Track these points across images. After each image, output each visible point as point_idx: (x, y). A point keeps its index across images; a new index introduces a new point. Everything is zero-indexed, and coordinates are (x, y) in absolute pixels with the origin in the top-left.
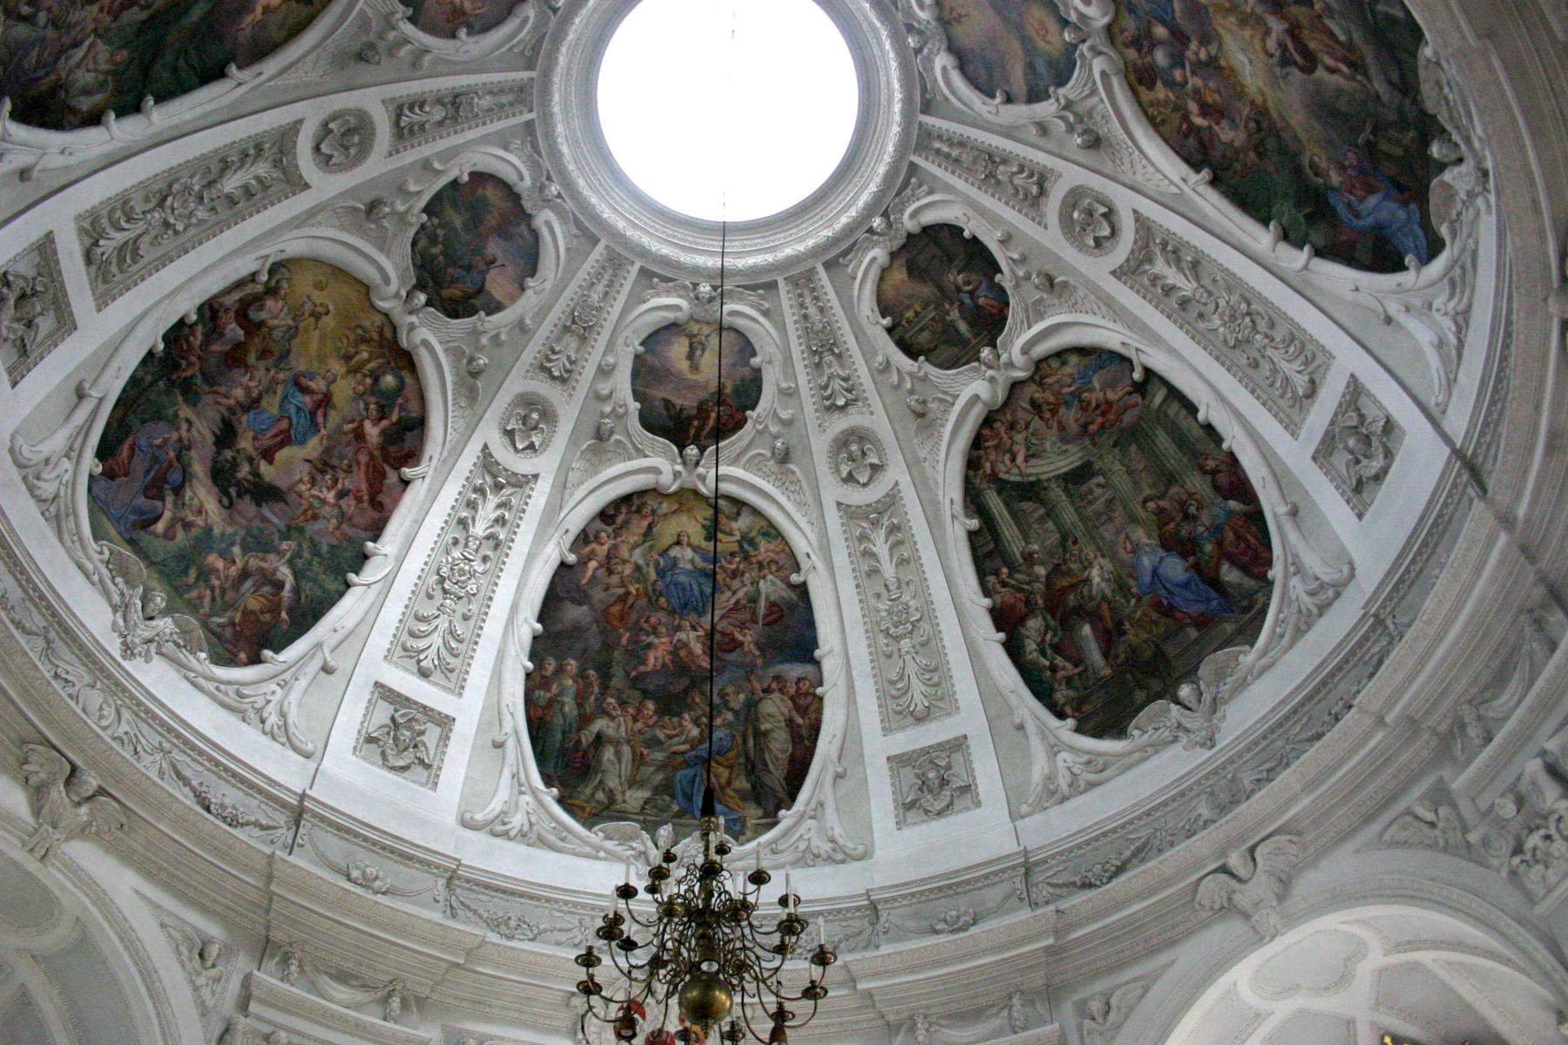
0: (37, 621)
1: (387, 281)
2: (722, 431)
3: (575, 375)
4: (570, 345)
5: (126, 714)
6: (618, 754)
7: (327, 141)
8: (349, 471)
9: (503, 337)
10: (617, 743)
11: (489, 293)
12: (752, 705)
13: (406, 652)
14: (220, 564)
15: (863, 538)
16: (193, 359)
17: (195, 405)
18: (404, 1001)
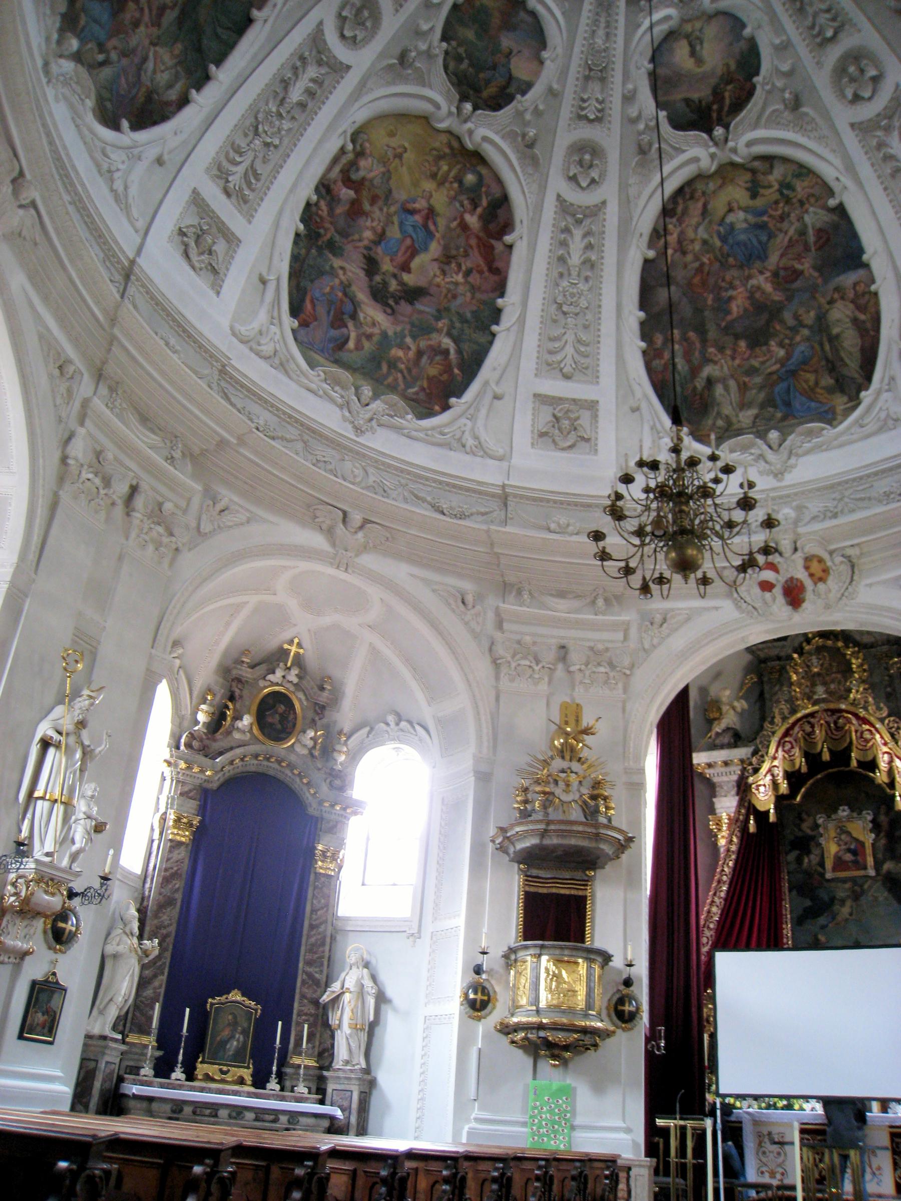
0: (292, 432)
1: (438, 107)
2: (738, 106)
3: (608, 111)
4: (595, 88)
5: (371, 470)
6: (727, 388)
7: (347, 26)
8: (466, 255)
9: (541, 107)
10: (723, 380)
11: (518, 79)
12: (821, 318)
13: (550, 365)
14: (400, 353)
15: (880, 145)
16: (327, 225)
17: (342, 255)
18: (606, 600)
